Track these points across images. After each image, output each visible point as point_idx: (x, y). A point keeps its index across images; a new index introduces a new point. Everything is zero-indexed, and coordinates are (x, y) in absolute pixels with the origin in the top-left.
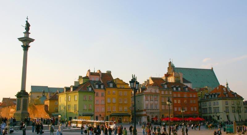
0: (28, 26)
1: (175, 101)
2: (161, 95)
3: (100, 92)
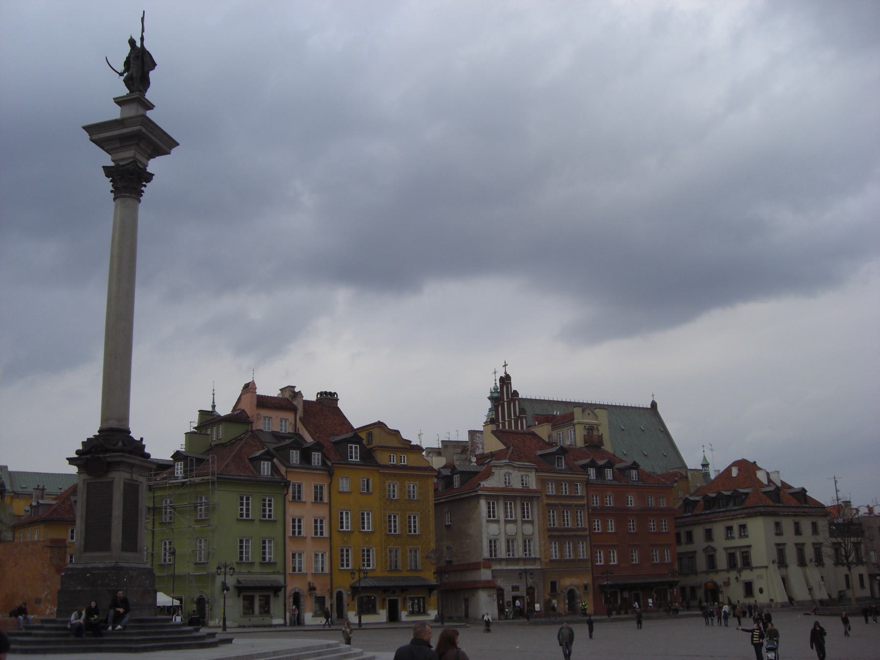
1: (598, 525)
2: (545, 501)
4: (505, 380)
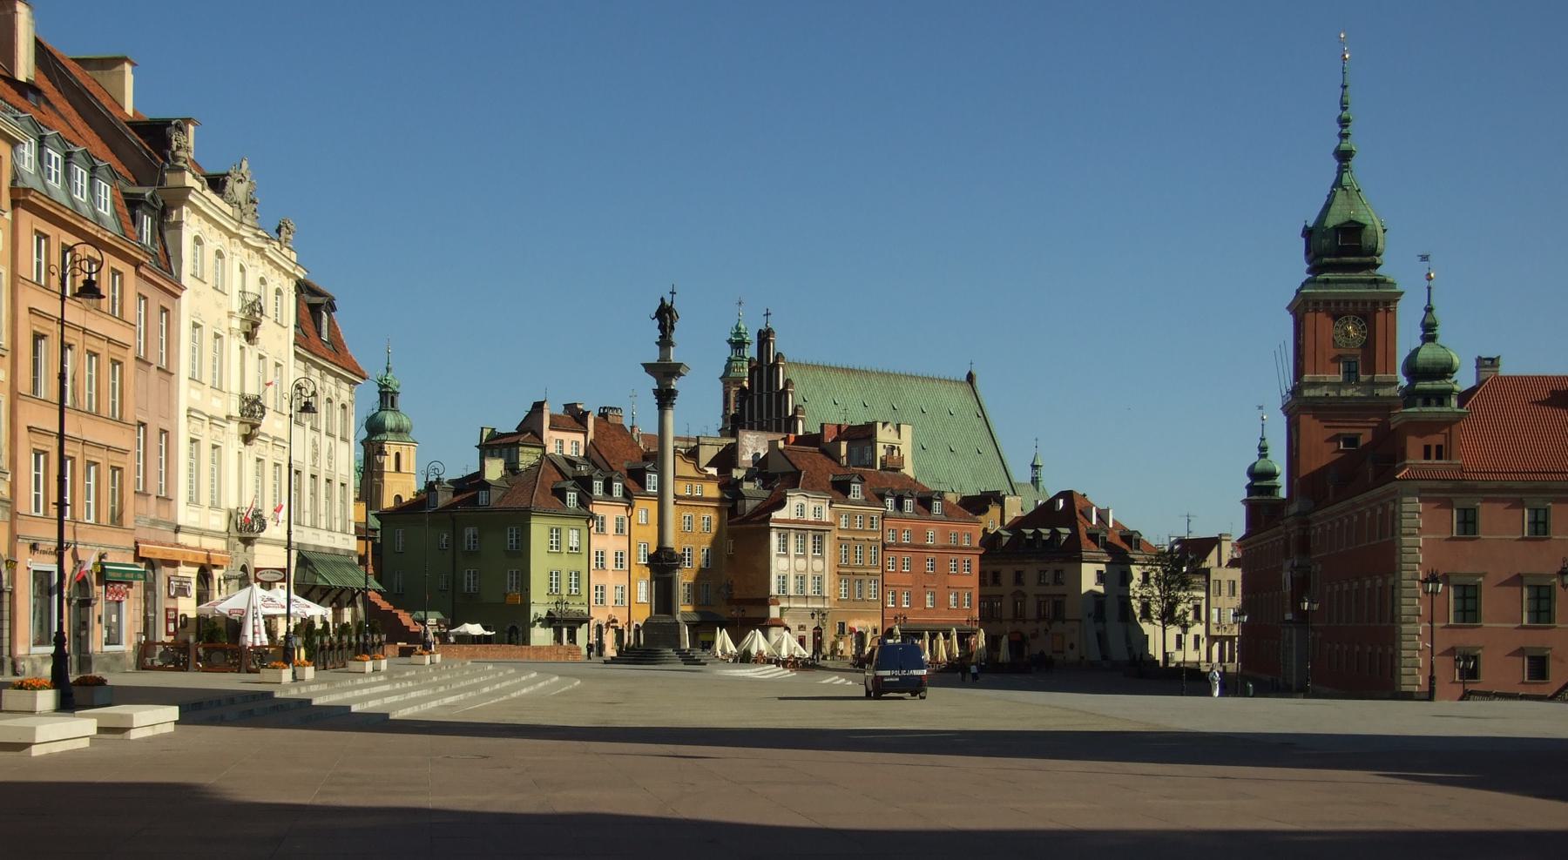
0: (665, 315)
3: (609, 512)
4: (764, 337)
